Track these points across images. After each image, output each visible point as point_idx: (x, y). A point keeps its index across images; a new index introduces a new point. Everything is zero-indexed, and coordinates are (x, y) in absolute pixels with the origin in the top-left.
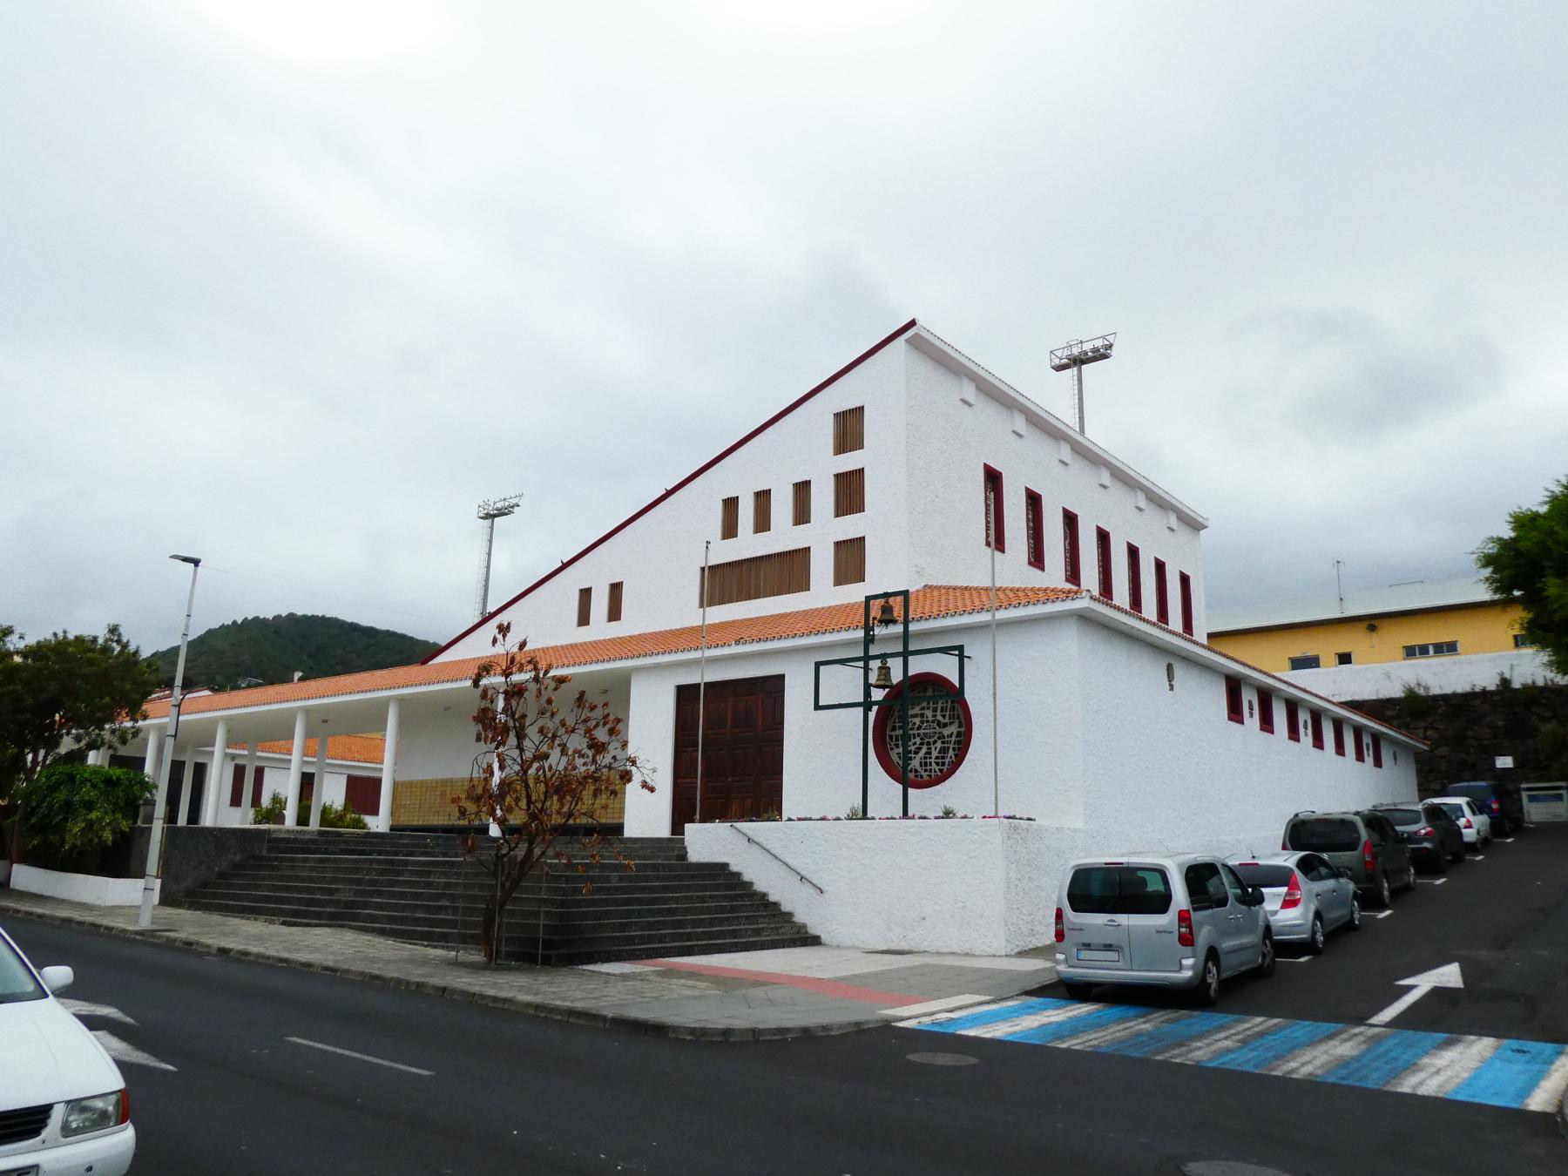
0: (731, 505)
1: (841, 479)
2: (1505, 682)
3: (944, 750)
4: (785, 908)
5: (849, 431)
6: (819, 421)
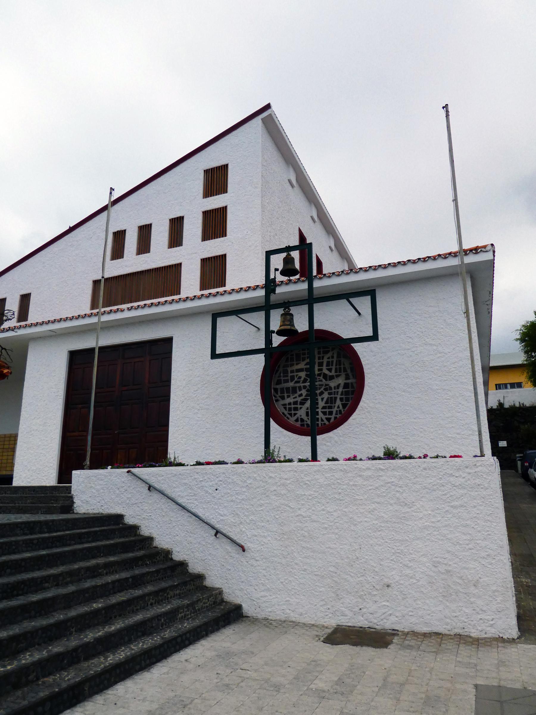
0: (119, 237)
1: (207, 215)
2: (501, 405)
3: (331, 401)
4: (195, 567)
5: (216, 180)
6: (194, 175)
